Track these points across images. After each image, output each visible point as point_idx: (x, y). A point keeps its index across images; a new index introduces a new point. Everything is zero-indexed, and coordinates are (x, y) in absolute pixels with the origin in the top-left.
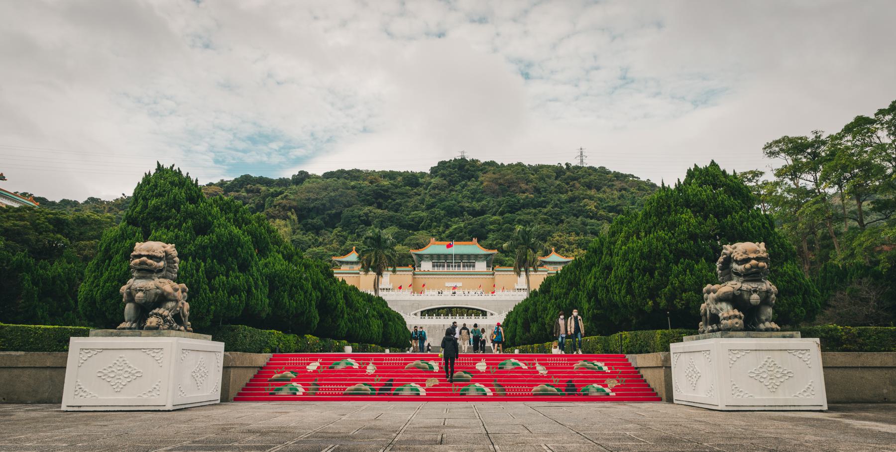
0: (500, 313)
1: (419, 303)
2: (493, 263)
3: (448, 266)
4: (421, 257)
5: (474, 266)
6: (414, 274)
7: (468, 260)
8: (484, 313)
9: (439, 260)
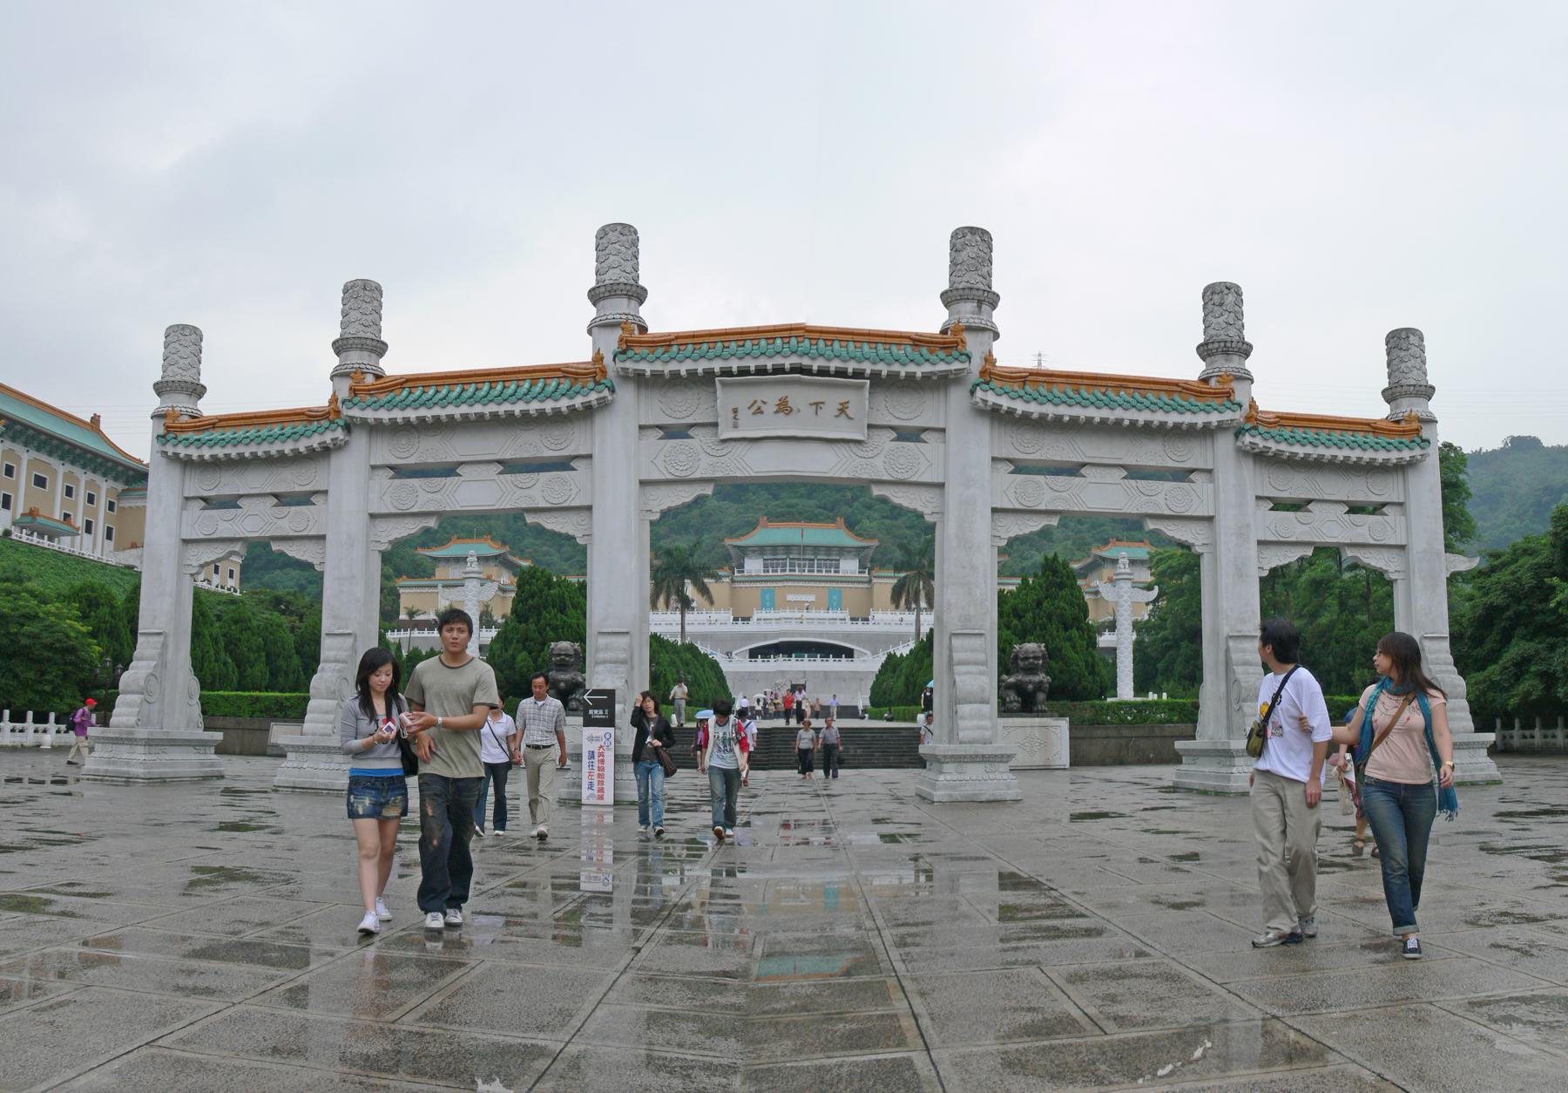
0: (875, 653)
1: (750, 637)
2: (872, 563)
3: (792, 565)
4: (744, 551)
5: (837, 567)
6: (733, 581)
8: (849, 653)
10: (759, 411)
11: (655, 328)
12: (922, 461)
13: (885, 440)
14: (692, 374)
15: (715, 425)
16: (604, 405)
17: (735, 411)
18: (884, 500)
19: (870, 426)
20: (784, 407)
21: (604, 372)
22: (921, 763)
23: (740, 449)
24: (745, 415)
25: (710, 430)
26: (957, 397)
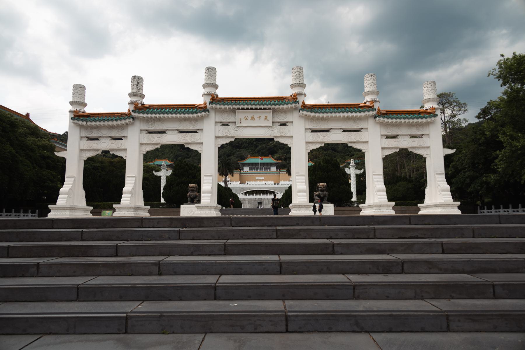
1: (244, 189)
6: (240, 173)
7: (267, 166)
9: (253, 166)
10: (247, 119)
11: (220, 96)
13: (277, 127)
15: (235, 122)
17: (241, 119)
19: (273, 122)
20: (253, 118)
21: (206, 107)
23: (241, 129)
24: (243, 120)
25: (234, 124)
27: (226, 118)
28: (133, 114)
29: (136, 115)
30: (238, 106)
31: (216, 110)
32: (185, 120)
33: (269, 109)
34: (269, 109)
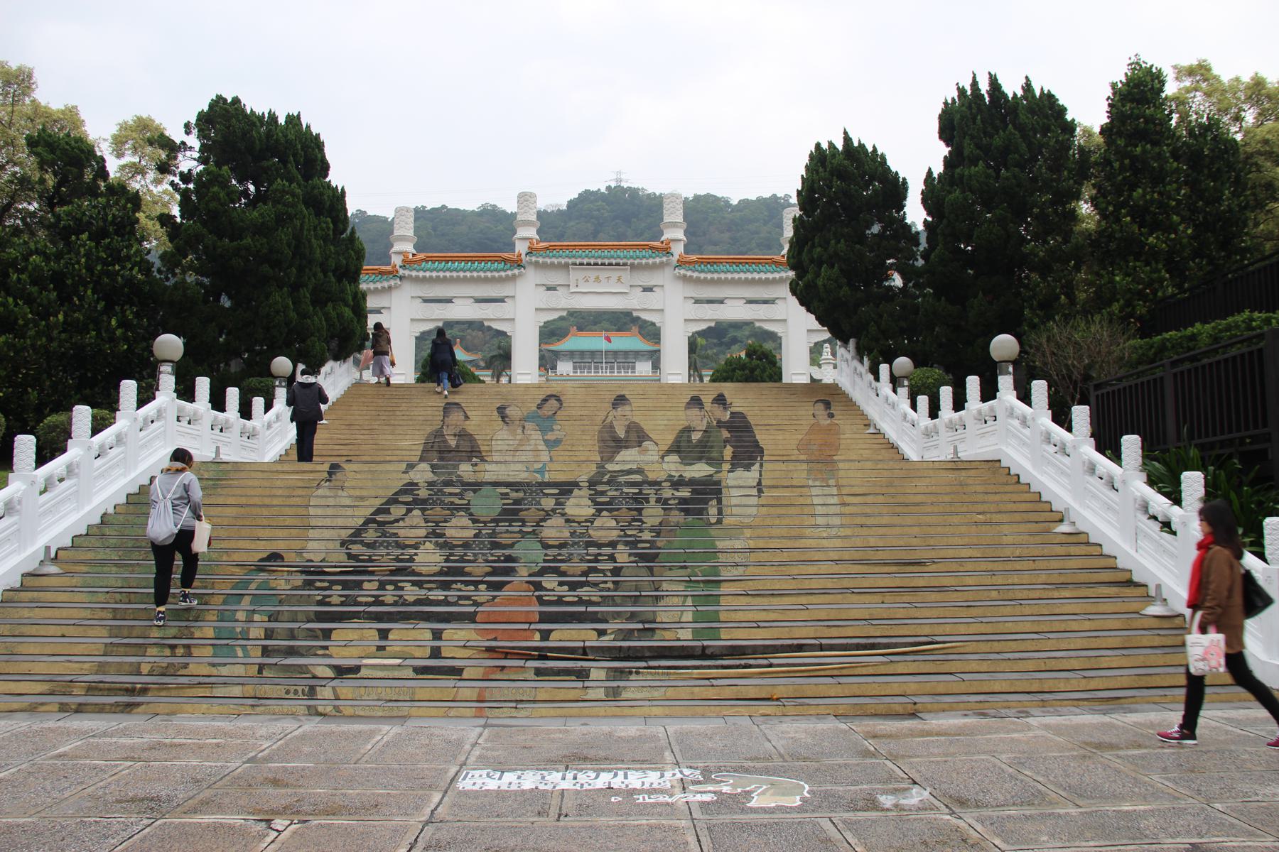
3: (596, 368)
5: (634, 368)
12: (652, 300)
14: (560, 264)
16: (520, 275)
18: (638, 318)
20: (597, 279)
22: (669, 452)
23: (578, 297)
24: (581, 282)
26: (668, 272)
27: (554, 278)
28: (401, 272)
29: (407, 273)
30: (573, 260)
31: (537, 264)
32: (486, 280)
33: (625, 265)
34: (625, 265)
